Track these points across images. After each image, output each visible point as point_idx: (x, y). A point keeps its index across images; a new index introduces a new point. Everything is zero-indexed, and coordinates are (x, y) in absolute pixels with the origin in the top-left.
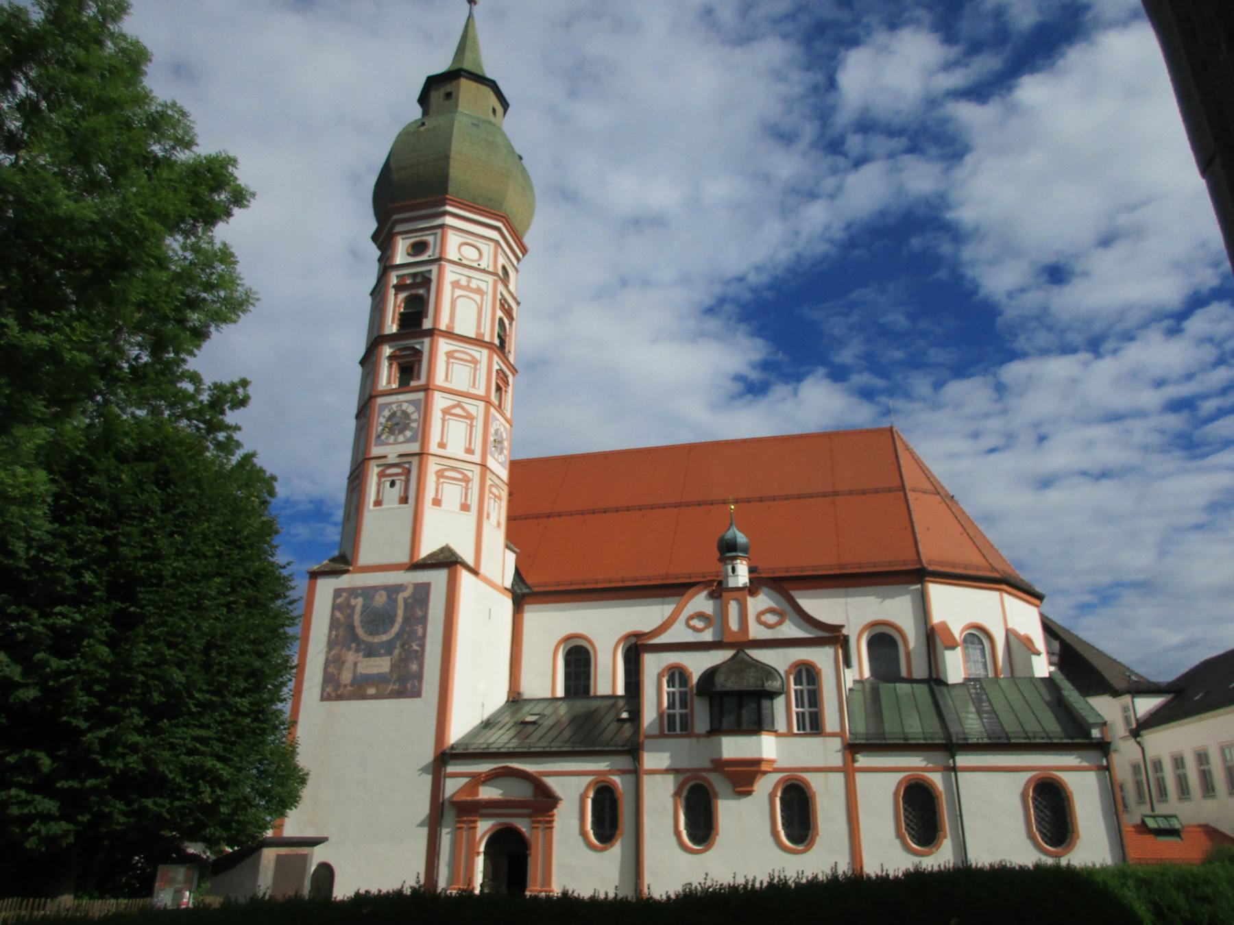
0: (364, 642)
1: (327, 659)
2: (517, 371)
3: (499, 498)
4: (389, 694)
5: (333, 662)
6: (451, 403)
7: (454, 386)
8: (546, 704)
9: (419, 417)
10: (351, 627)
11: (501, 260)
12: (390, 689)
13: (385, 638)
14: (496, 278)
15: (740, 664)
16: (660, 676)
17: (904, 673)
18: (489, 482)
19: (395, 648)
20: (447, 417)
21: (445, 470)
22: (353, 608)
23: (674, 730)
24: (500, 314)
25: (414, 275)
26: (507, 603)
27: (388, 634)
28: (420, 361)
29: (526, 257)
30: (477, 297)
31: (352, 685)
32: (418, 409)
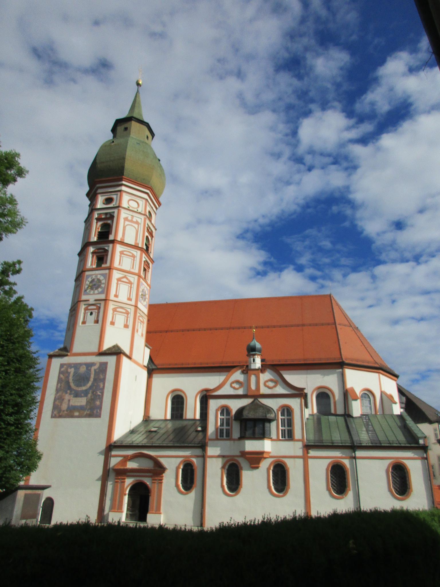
0: (74, 390)
1: (55, 398)
2: (154, 262)
3: (143, 322)
6: (121, 276)
7: (123, 267)
8: (162, 422)
9: (106, 281)
10: (68, 383)
11: (148, 208)
12: (85, 413)
13: (84, 388)
14: (145, 217)
15: (255, 406)
16: (217, 411)
17: (333, 411)
18: (138, 315)
19: (89, 393)
20: (119, 282)
21: (117, 308)
22: (69, 373)
23: (223, 437)
24: (147, 234)
25: (106, 214)
26: (145, 373)
28: (107, 255)
29: (160, 208)
30: (136, 226)
31: (67, 411)
32: (105, 278)
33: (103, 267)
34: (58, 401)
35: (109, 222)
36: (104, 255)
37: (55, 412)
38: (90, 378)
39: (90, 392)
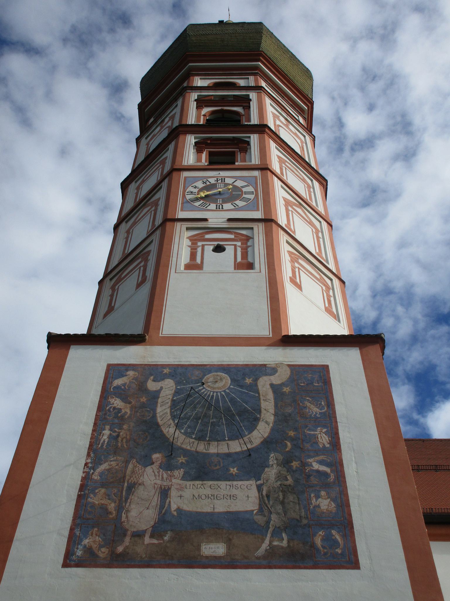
0: (186, 453)
4: (264, 557)
5: (103, 485)
12: (265, 545)
22: (155, 396)
39: (272, 461)
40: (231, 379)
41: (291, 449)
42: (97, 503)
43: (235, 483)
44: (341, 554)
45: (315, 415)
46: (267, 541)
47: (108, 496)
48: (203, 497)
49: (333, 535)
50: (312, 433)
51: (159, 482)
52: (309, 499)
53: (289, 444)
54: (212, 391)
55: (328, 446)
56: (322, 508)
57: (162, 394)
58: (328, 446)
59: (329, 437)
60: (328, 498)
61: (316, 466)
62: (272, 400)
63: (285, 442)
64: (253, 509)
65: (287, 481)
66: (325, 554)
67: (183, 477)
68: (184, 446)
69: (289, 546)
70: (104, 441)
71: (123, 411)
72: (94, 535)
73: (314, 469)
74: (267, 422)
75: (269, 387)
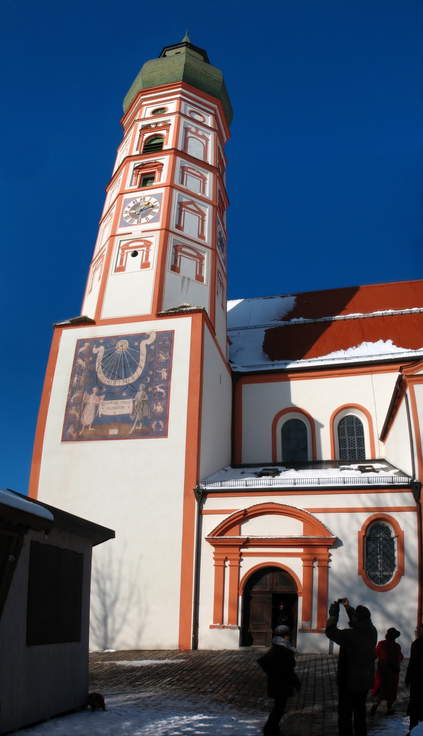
4: (132, 434)
9: (160, 205)
12: (133, 429)
22: (95, 356)
27: (130, 378)
28: (160, 170)
30: (204, 141)
31: (93, 425)
33: (155, 185)
34: (74, 407)
35: (164, 132)
36: (154, 173)
37: (71, 430)
38: (138, 361)
39: (141, 388)
40: (129, 343)
41: (150, 381)
42: (72, 413)
43: (124, 400)
44: (162, 432)
45: (163, 362)
46: (134, 428)
47: (76, 410)
48: (111, 408)
49: (160, 423)
50: (160, 371)
51: (95, 402)
52: (153, 407)
53: (149, 379)
54: (119, 351)
55: (165, 378)
56: (158, 411)
57: (99, 355)
58: (165, 378)
59: (167, 374)
60: (161, 405)
61: (159, 390)
62: (145, 355)
63: (148, 378)
64: (130, 413)
65: (145, 398)
66: (155, 432)
67: (104, 399)
68: (106, 383)
69: (142, 429)
70: (75, 383)
71: (83, 366)
72: (71, 428)
73: (158, 391)
74: (141, 368)
75: (145, 346)
